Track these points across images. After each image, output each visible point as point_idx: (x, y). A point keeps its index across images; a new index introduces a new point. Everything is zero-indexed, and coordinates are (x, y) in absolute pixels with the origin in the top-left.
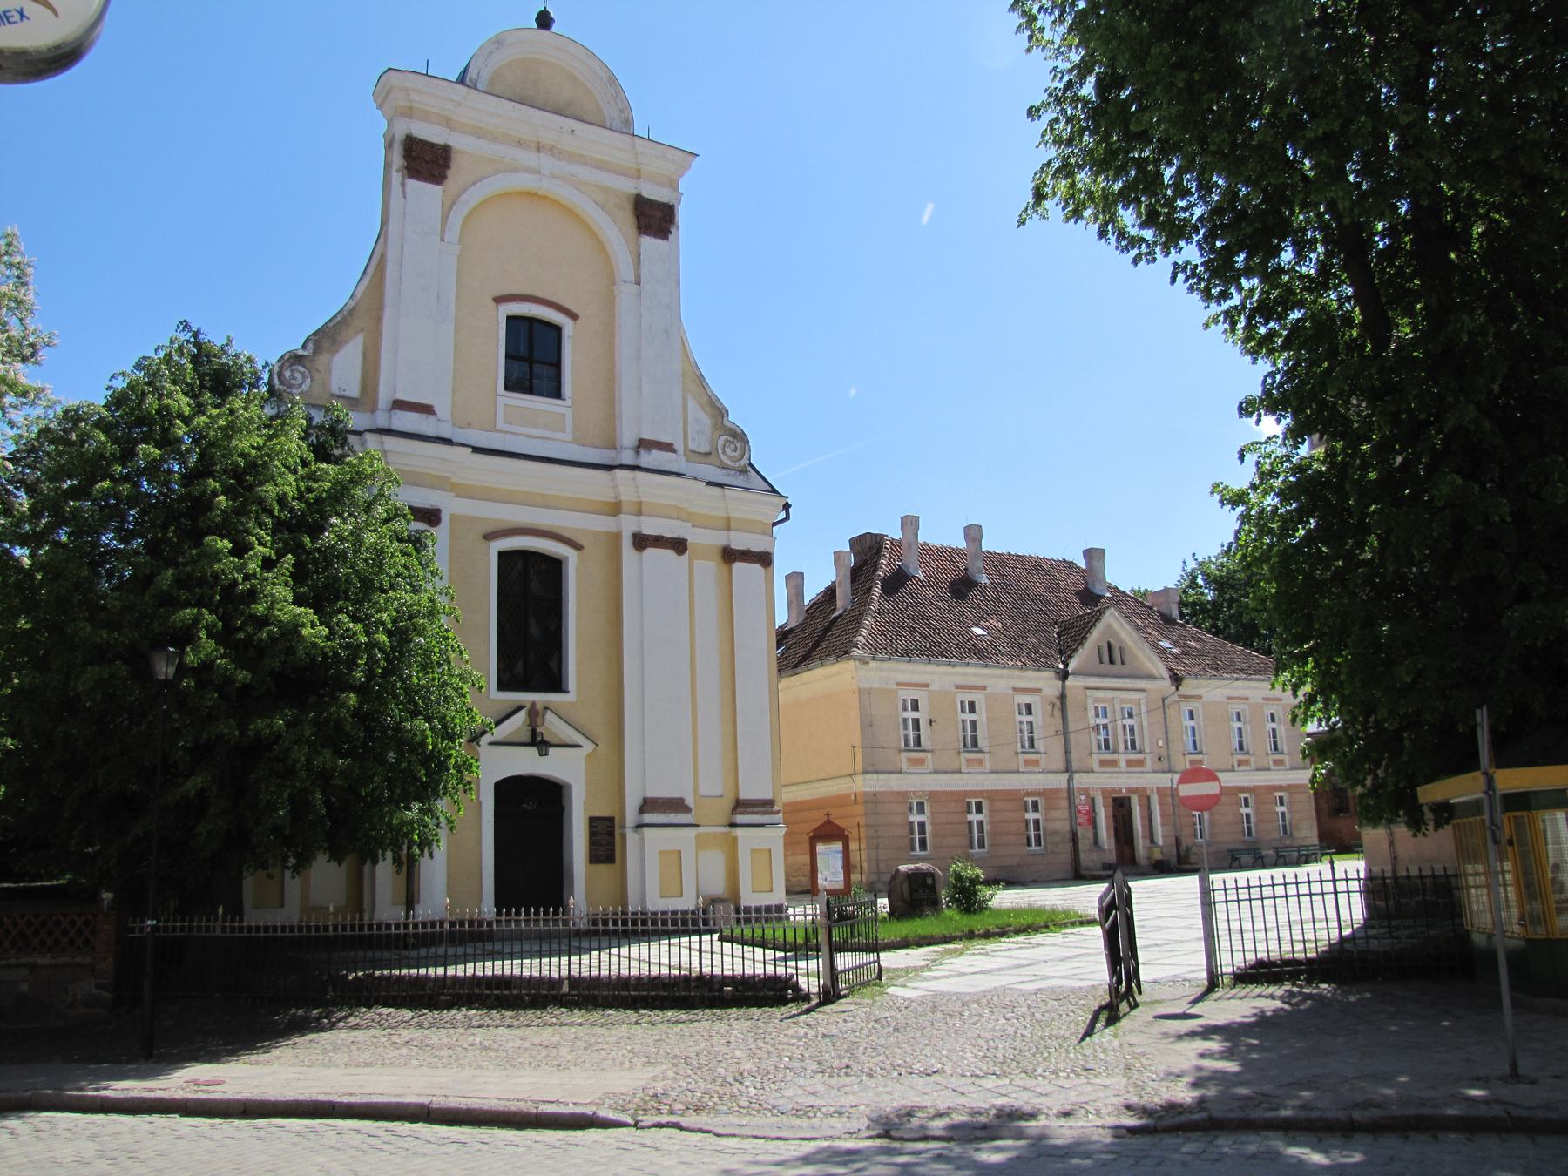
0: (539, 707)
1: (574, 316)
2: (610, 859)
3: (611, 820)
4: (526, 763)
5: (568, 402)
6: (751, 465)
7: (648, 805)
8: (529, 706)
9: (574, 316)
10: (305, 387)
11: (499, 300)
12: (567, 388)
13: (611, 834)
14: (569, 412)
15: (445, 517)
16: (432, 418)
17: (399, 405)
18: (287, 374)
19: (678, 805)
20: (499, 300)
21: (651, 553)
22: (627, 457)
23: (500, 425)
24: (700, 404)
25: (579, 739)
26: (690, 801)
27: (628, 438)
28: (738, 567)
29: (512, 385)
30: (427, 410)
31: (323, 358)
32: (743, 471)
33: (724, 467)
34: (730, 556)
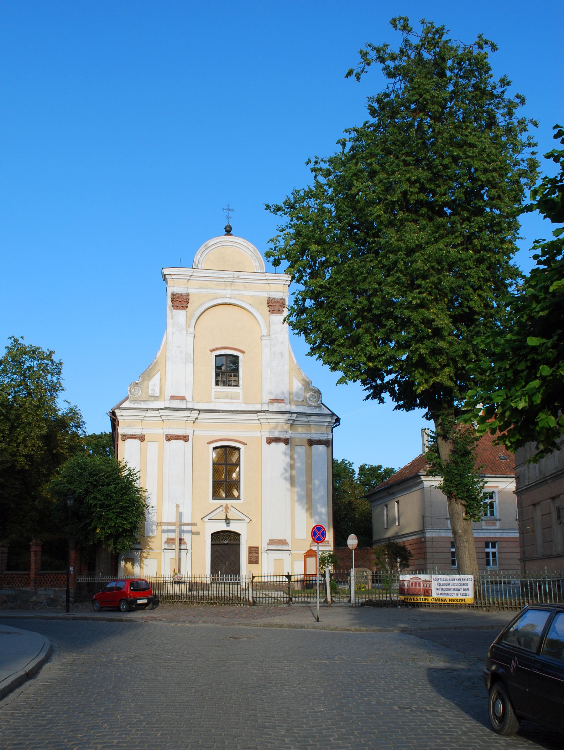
0: (229, 506)
1: (243, 352)
2: (257, 562)
3: (257, 548)
4: (222, 526)
5: (241, 387)
6: (322, 403)
7: (272, 542)
8: (224, 506)
9: (243, 352)
10: (139, 394)
11: (212, 351)
12: (241, 382)
13: (257, 553)
14: (241, 391)
15: (190, 438)
16: (185, 401)
17: (173, 398)
18: (133, 390)
19: (283, 542)
20: (212, 351)
21: (273, 444)
22: (265, 408)
23: (213, 400)
24: (299, 381)
25: (244, 518)
26: (289, 541)
27: (266, 398)
28: (314, 447)
29: (217, 384)
30: (182, 398)
31: (146, 383)
32: (319, 407)
33: (309, 406)
34: (311, 443)
